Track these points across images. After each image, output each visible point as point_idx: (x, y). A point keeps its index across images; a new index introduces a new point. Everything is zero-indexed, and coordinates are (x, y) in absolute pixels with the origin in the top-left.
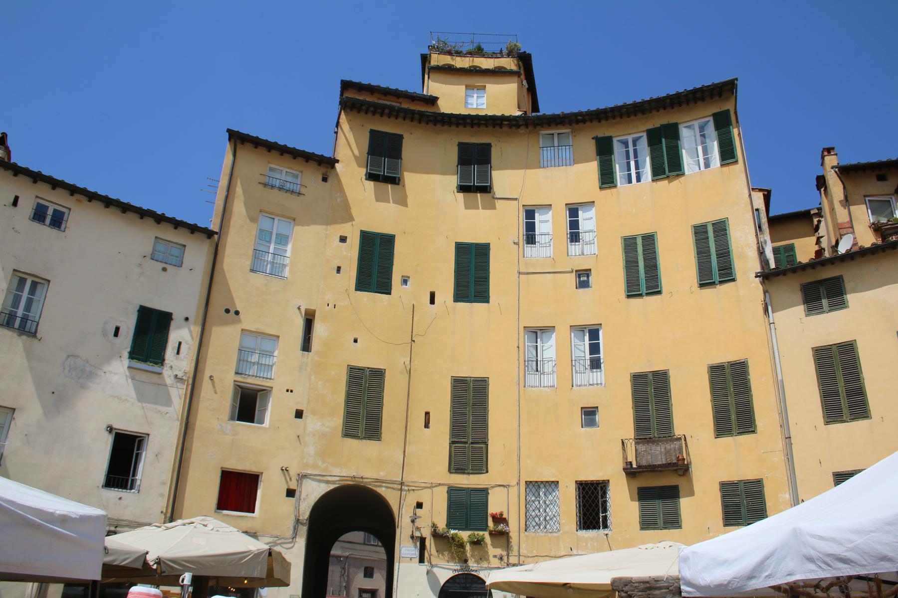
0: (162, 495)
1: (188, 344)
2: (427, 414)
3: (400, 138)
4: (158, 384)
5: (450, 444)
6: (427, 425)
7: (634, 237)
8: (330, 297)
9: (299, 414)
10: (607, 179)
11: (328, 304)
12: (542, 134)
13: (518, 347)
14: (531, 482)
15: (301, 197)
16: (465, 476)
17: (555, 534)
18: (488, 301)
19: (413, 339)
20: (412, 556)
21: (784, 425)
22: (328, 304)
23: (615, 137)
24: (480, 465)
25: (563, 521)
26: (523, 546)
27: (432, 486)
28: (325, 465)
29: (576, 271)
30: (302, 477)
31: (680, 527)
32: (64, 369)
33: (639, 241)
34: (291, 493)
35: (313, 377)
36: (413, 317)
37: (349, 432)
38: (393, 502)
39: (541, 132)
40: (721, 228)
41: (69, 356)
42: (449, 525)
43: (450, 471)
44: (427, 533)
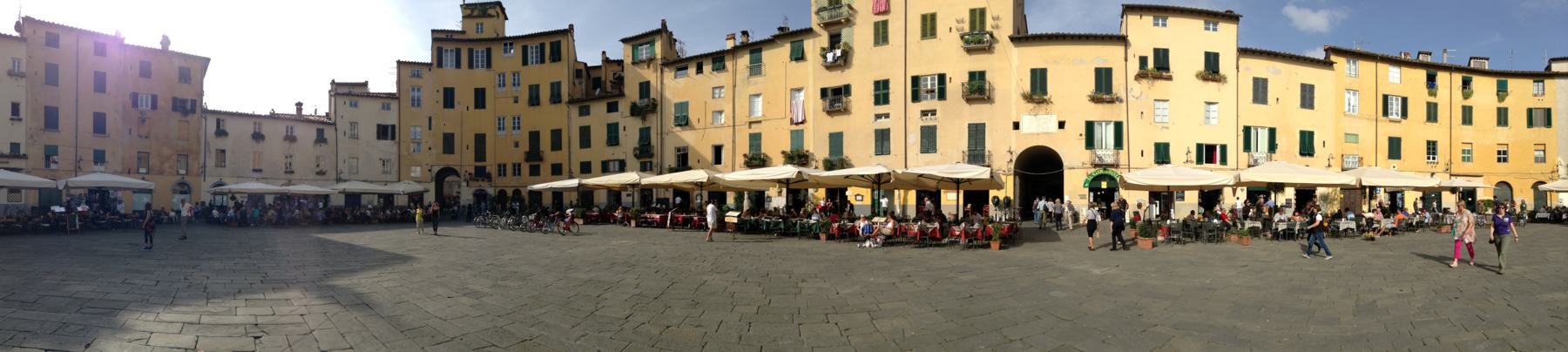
9: (430, 149)
10: (525, 62)
21: (569, 148)
24: (484, 160)
27: (470, 166)
30: (432, 166)
37: (445, 152)
40: (559, 84)
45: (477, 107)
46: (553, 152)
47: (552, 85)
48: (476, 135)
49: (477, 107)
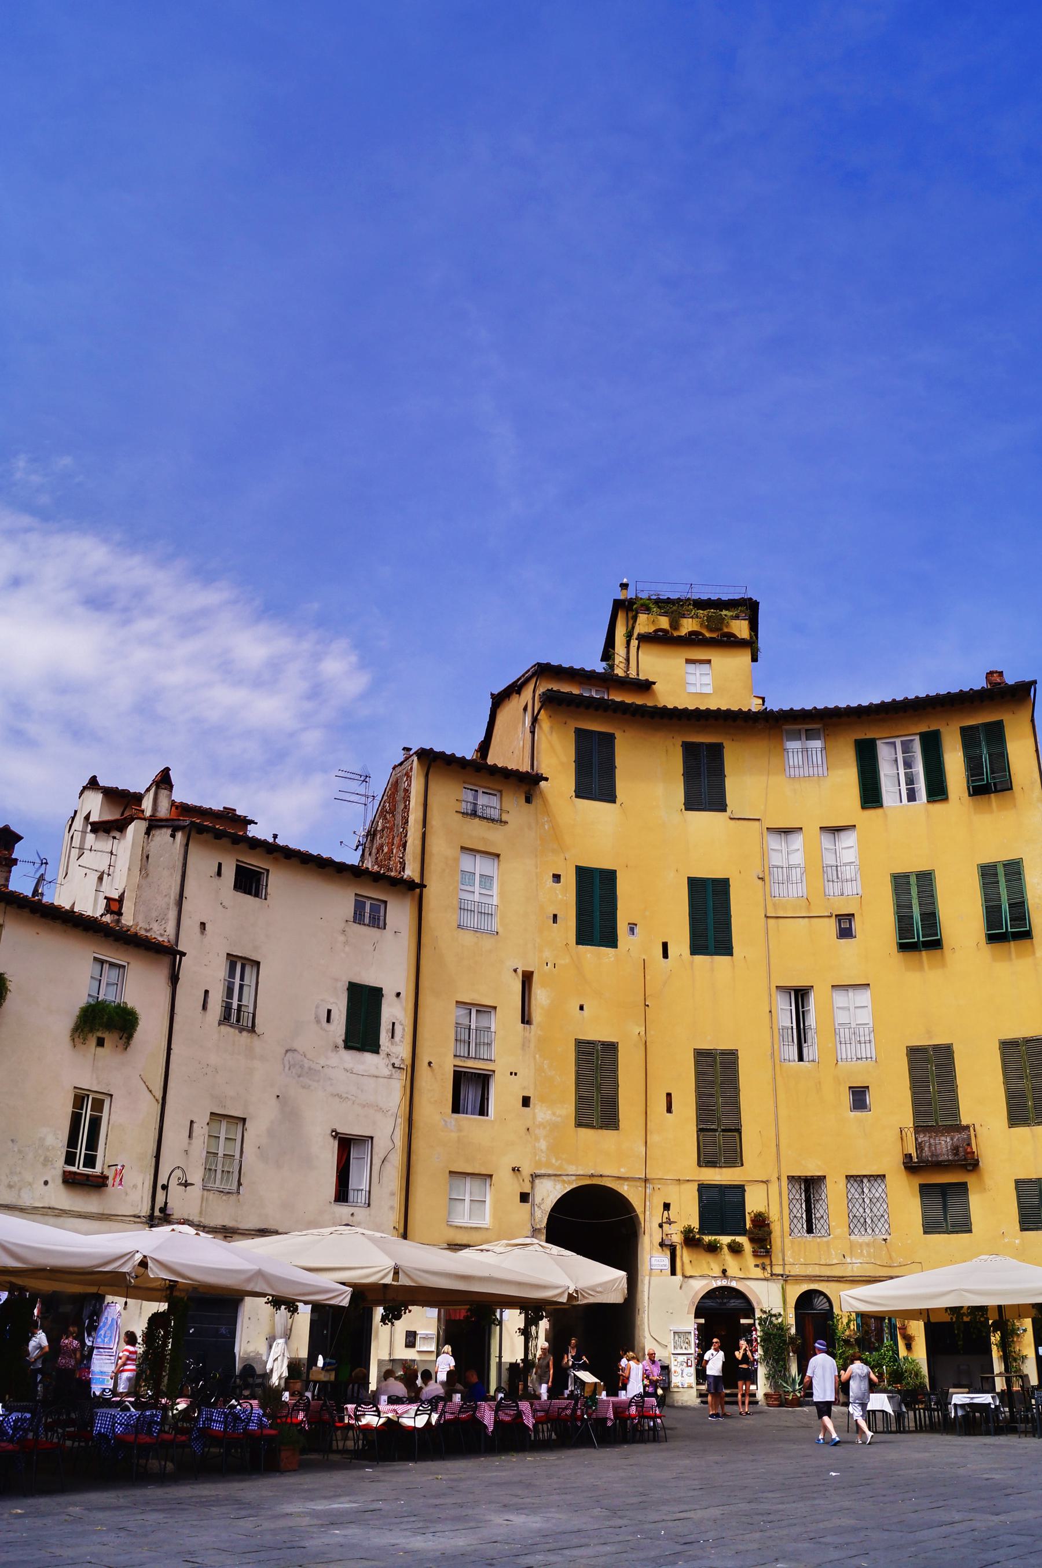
0: (392, 1208)
1: (402, 1025)
2: (669, 1095)
3: (610, 738)
4: (376, 1077)
5: (697, 1131)
6: (669, 1110)
7: (907, 874)
8: (547, 954)
9: (526, 1102)
11: (547, 963)
12: (787, 731)
13: (770, 1012)
14: (793, 1177)
15: (506, 827)
16: (717, 1170)
17: (825, 1239)
18: (731, 954)
19: (647, 1004)
20: (662, 1268)
22: (547, 963)
23: (878, 739)
24: (734, 1158)
25: (834, 1224)
26: (788, 1253)
28: (559, 1162)
29: (836, 916)
30: (534, 1177)
31: (970, 1231)
32: (284, 1067)
33: (913, 880)
34: (524, 1197)
35: (537, 1056)
36: (645, 976)
38: (636, 1203)
39: (785, 727)
41: (287, 1051)
42: (702, 1230)
43: (699, 1165)
44: (677, 1238)
45: (698, 947)
46: (1022, 1132)
47: (988, 873)
48: (703, 1057)
49: (698, 947)
